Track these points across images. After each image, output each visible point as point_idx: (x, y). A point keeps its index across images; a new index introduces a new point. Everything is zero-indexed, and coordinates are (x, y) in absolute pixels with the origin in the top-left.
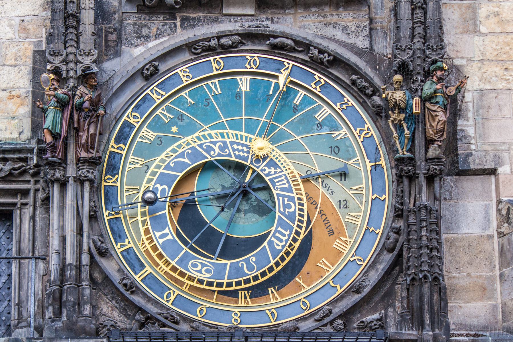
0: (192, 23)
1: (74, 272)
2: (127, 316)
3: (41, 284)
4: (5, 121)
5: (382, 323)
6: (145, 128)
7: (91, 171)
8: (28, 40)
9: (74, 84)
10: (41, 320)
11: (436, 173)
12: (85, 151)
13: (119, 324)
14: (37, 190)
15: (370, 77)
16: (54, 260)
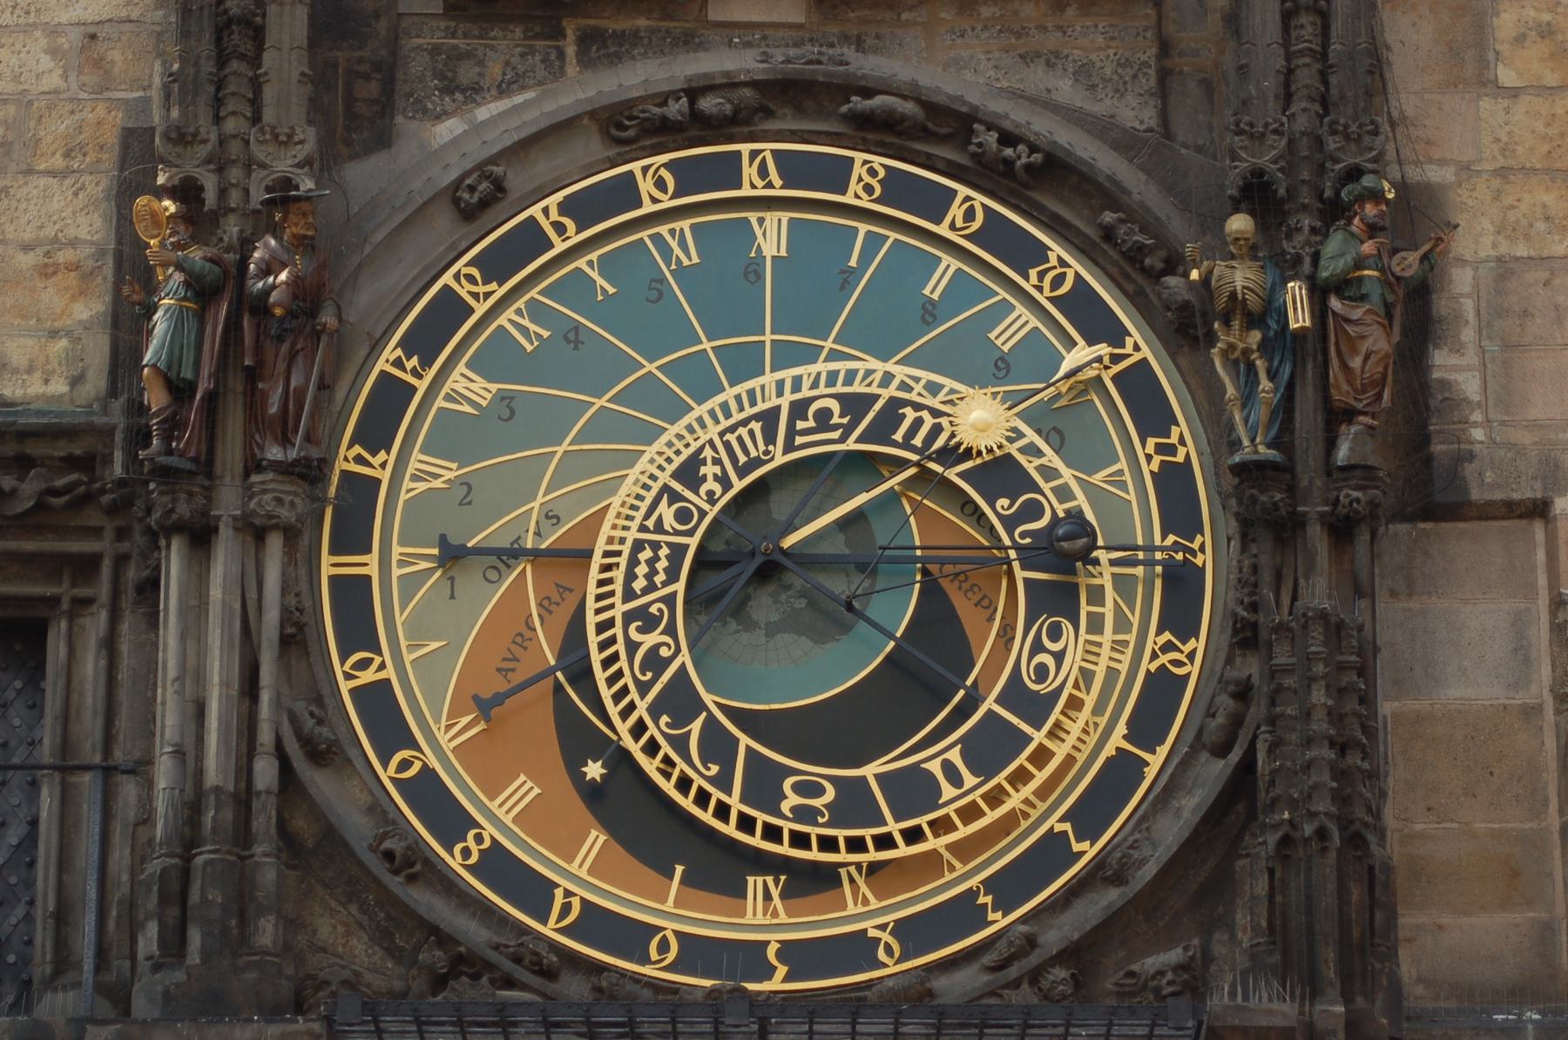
0: (612, 49)
1: (228, 815)
2: (392, 952)
3: (128, 851)
4: (30, 342)
5: (1194, 978)
6: (461, 367)
7: (288, 498)
8: (107, 95)
9: (242, 231)
10: (127, 963)
11: (1357, 512)
12: (276, 439)
13: (369, 977)
14: (121, 560)
15: (1157, 218)
16: (164, 774)
